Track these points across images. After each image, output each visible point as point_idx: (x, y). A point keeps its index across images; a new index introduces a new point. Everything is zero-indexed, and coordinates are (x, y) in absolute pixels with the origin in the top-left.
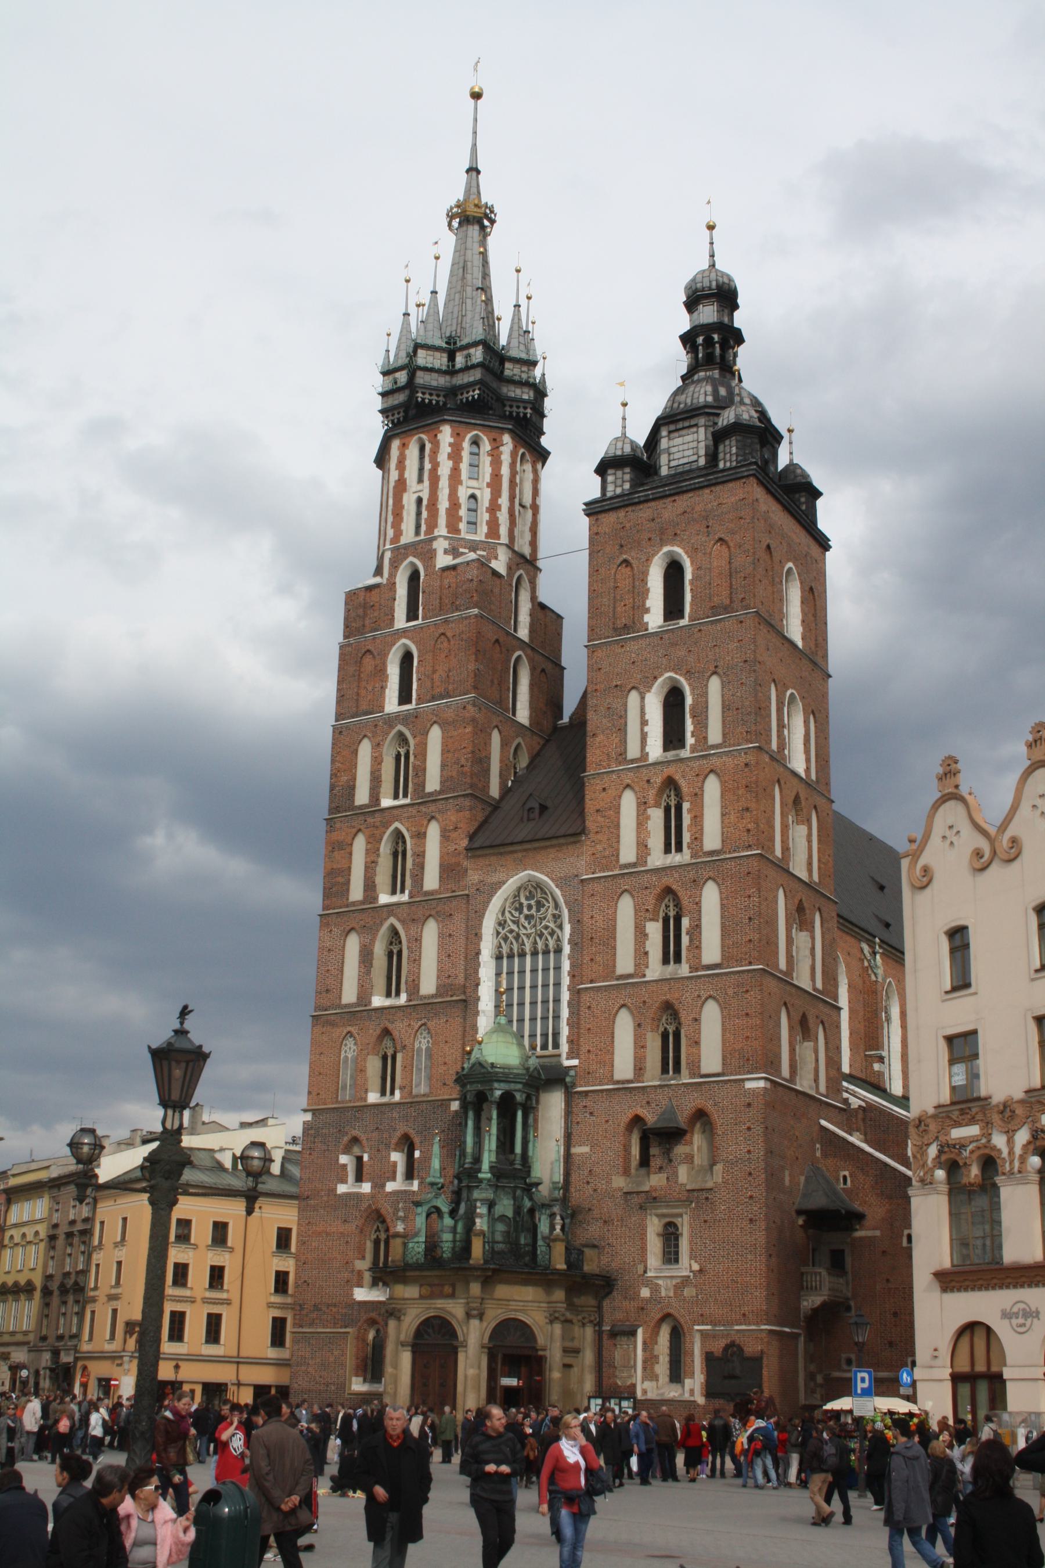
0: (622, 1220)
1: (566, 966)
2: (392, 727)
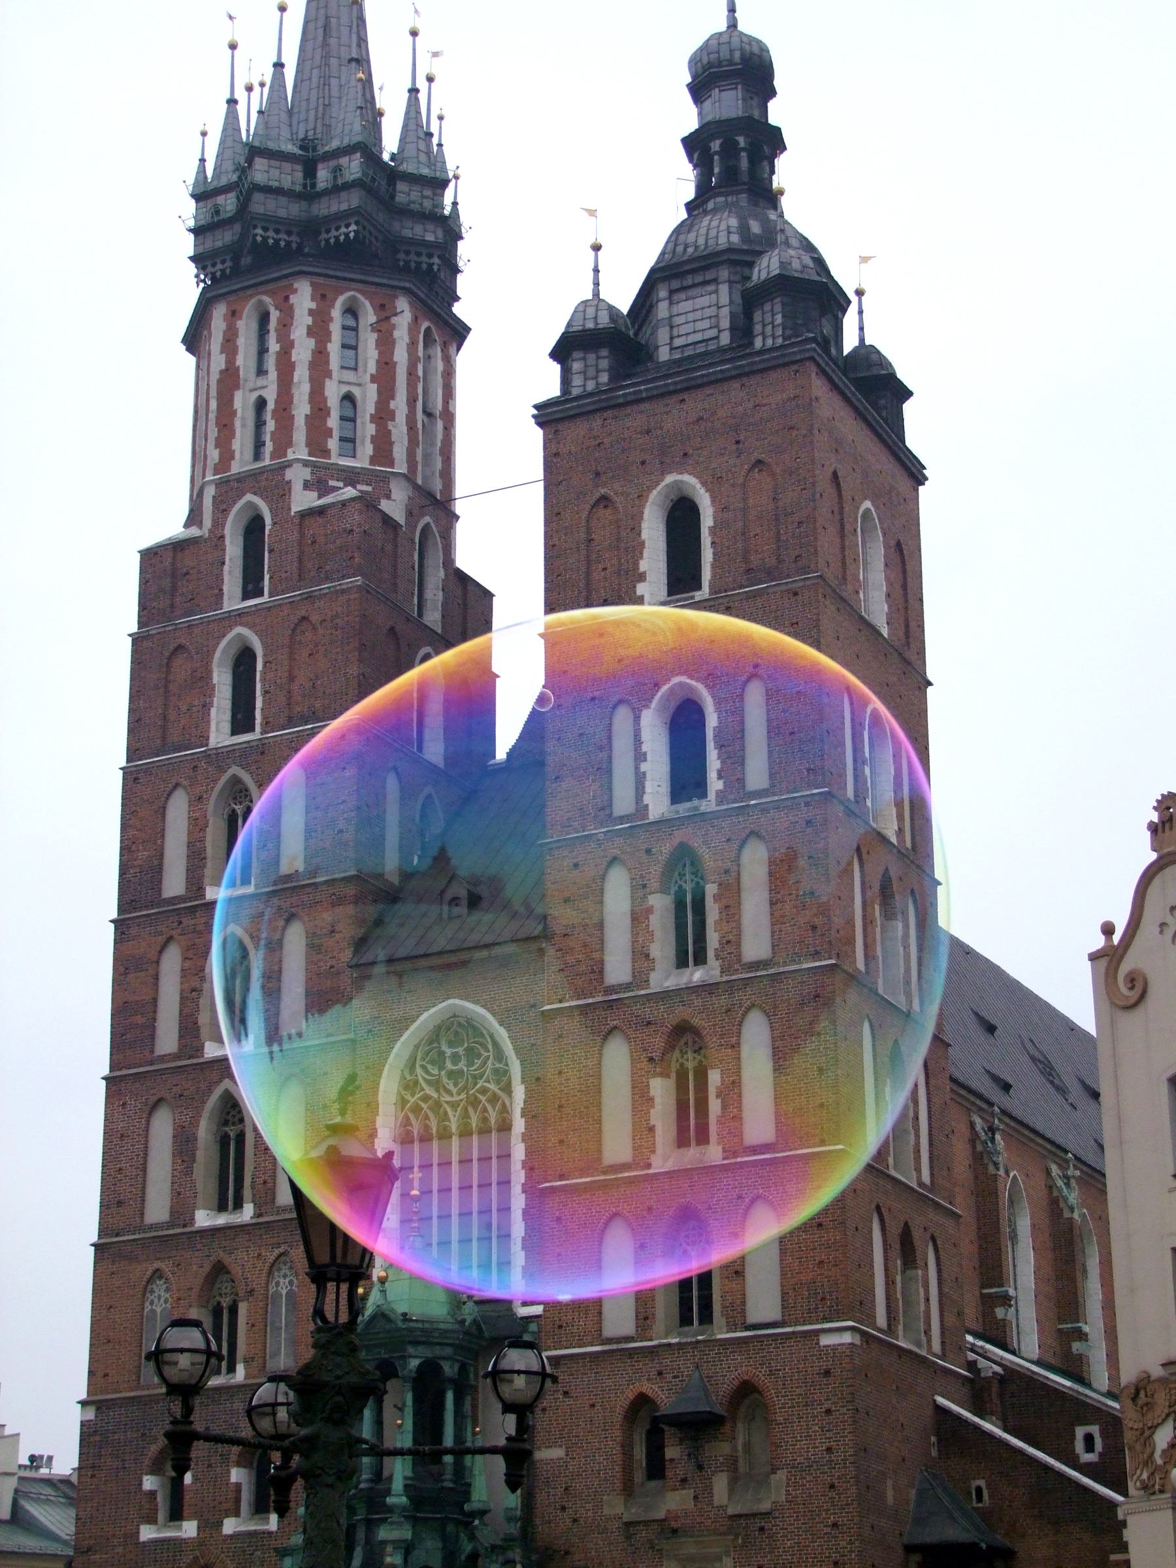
2: (222, 770)
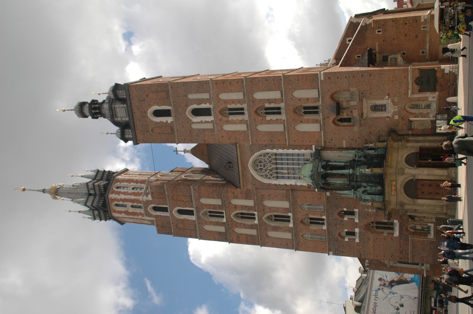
0: (370, 127)
1: (280, 151)
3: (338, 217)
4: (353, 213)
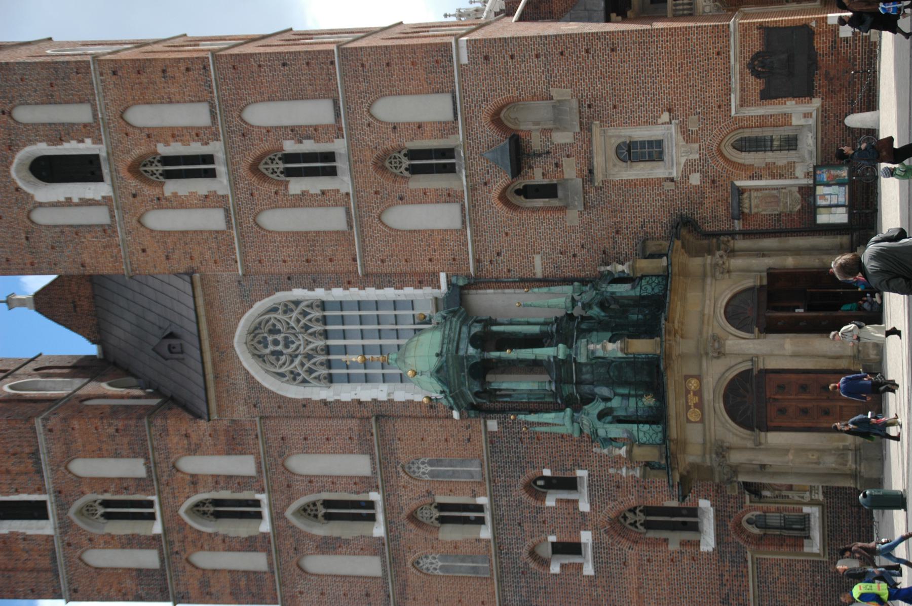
2: (71, 524)
3: (525, 497)
4: (571, 484)
